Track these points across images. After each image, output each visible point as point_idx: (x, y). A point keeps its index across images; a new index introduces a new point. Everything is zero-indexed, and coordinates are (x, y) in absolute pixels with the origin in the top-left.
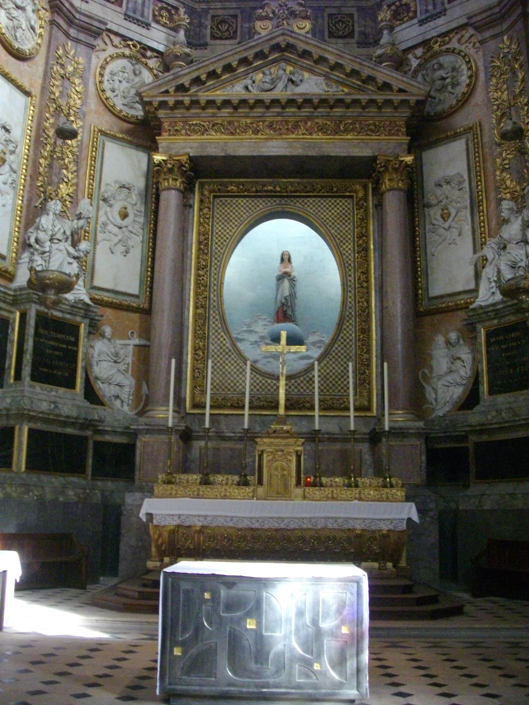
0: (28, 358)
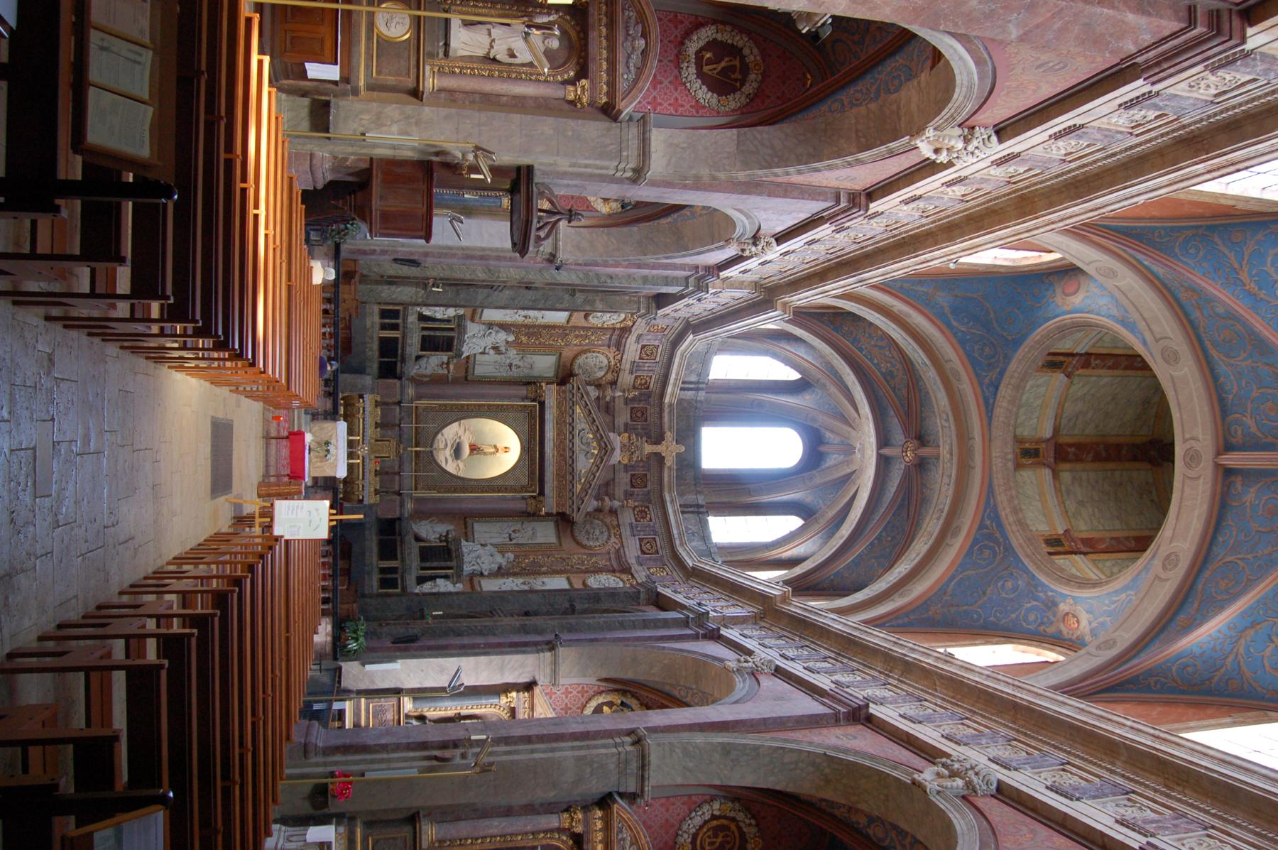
0: (432, 333)
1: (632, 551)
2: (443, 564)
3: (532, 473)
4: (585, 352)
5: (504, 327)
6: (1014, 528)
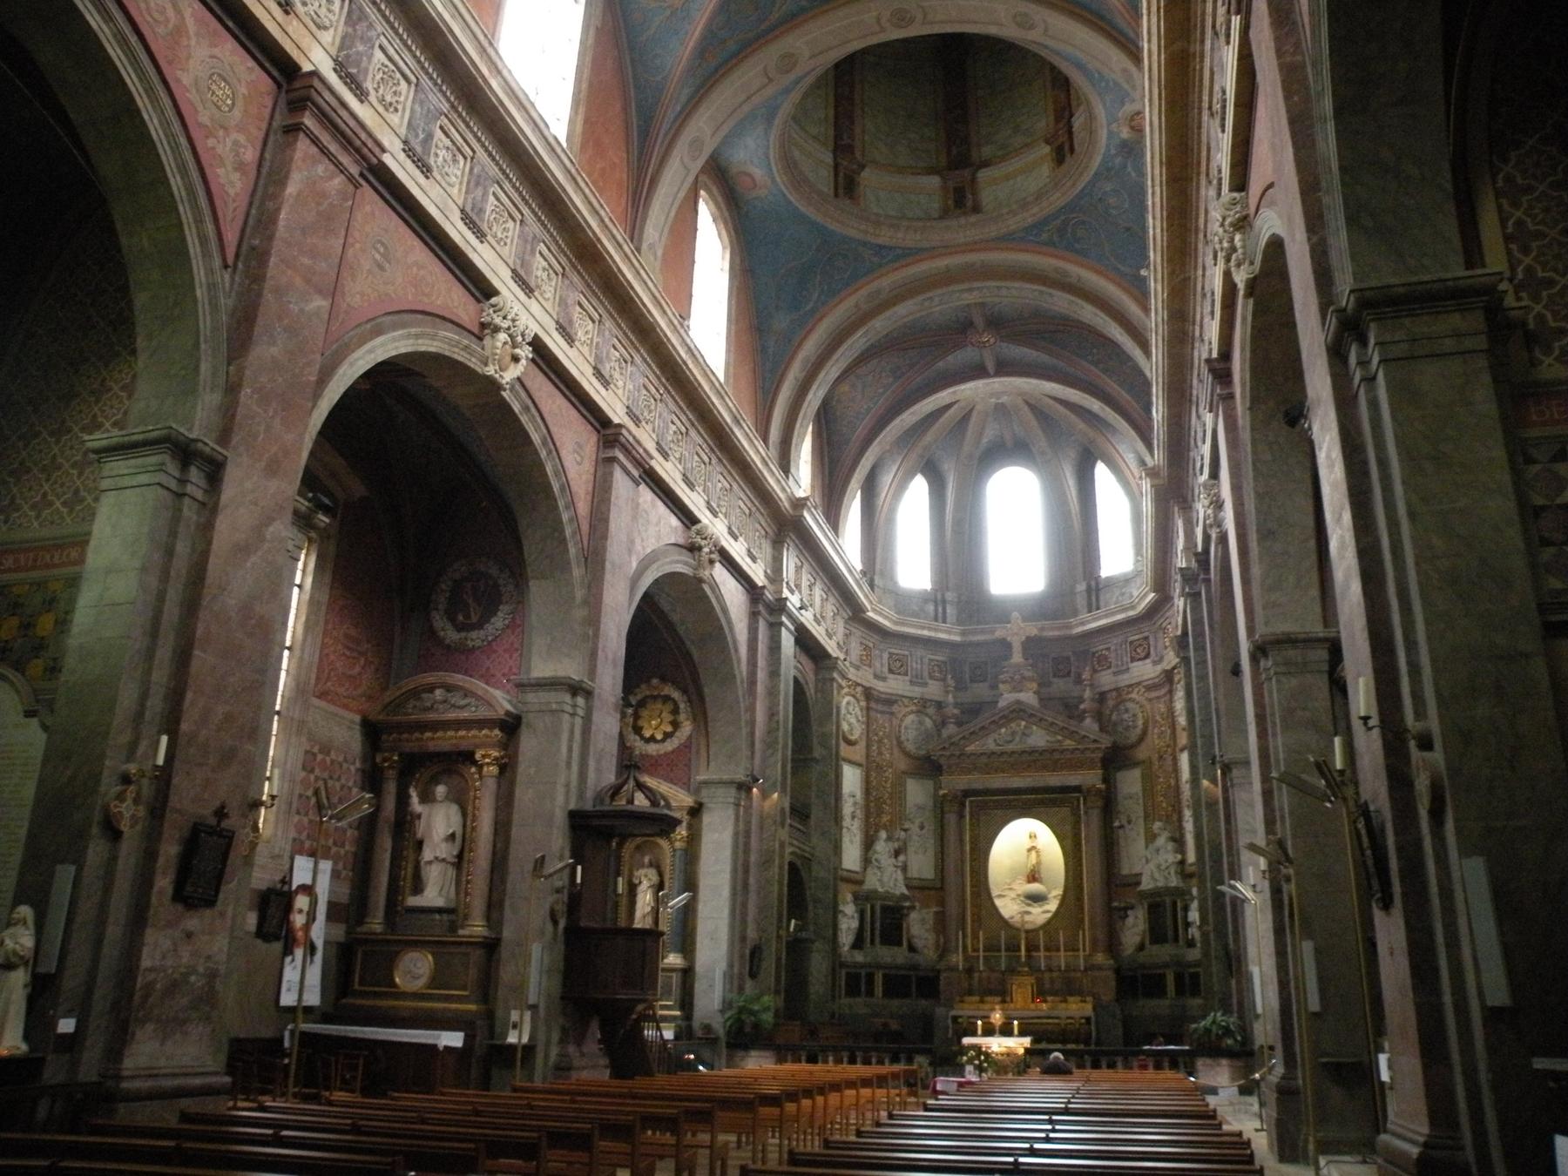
0: (877, 932)
1: (1146, 671)
2: (1169, 914)
3: (1054, 803)
4: (900, 743)
5: (868, 844)
6: (1044, 204)
